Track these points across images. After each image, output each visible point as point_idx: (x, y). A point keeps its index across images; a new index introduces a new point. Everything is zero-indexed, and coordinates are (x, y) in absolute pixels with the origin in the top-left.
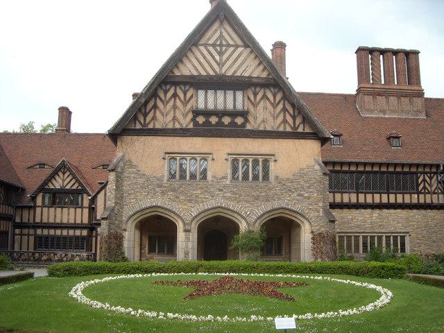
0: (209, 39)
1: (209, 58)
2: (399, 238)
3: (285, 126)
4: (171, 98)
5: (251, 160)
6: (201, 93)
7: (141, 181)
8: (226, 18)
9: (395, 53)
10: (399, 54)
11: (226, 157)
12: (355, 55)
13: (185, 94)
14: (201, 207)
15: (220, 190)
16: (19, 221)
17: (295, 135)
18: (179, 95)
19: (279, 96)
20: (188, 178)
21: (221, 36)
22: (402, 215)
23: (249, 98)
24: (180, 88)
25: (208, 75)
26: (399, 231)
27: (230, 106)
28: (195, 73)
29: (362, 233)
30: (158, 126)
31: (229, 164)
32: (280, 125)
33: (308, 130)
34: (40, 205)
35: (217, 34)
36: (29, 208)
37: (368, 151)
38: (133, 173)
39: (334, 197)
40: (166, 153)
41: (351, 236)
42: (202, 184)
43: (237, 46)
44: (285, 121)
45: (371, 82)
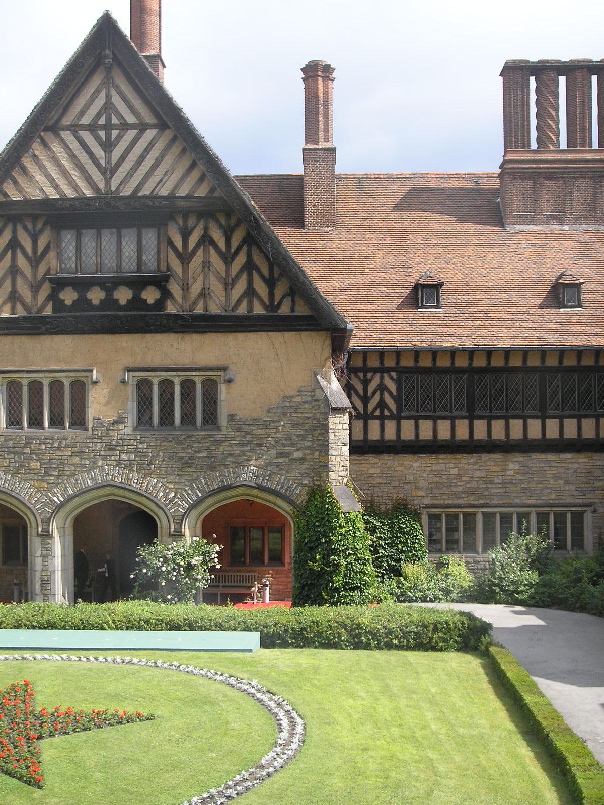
0: (82, 113)
1: (83, 157)
2: (569, 515)
3: (250, 304)
6: (68, 238)
12: (501, 78)
15: (110, 450)
17: (272, 323)
18: (23, 243)
21: (108, 107)
22: (576, 466)
23: (171, 243)
24: (25, 228)
25: (82, 199)
26: (569, 500)
27: (129, 265)
29: (482, 506)
31: (131, 392)
32: (239, 302)
33: (302, 310)
37: (500, 320)
39: (417, 427)
41: (456, 516)
43: (143, 127)
44: (250, 293)
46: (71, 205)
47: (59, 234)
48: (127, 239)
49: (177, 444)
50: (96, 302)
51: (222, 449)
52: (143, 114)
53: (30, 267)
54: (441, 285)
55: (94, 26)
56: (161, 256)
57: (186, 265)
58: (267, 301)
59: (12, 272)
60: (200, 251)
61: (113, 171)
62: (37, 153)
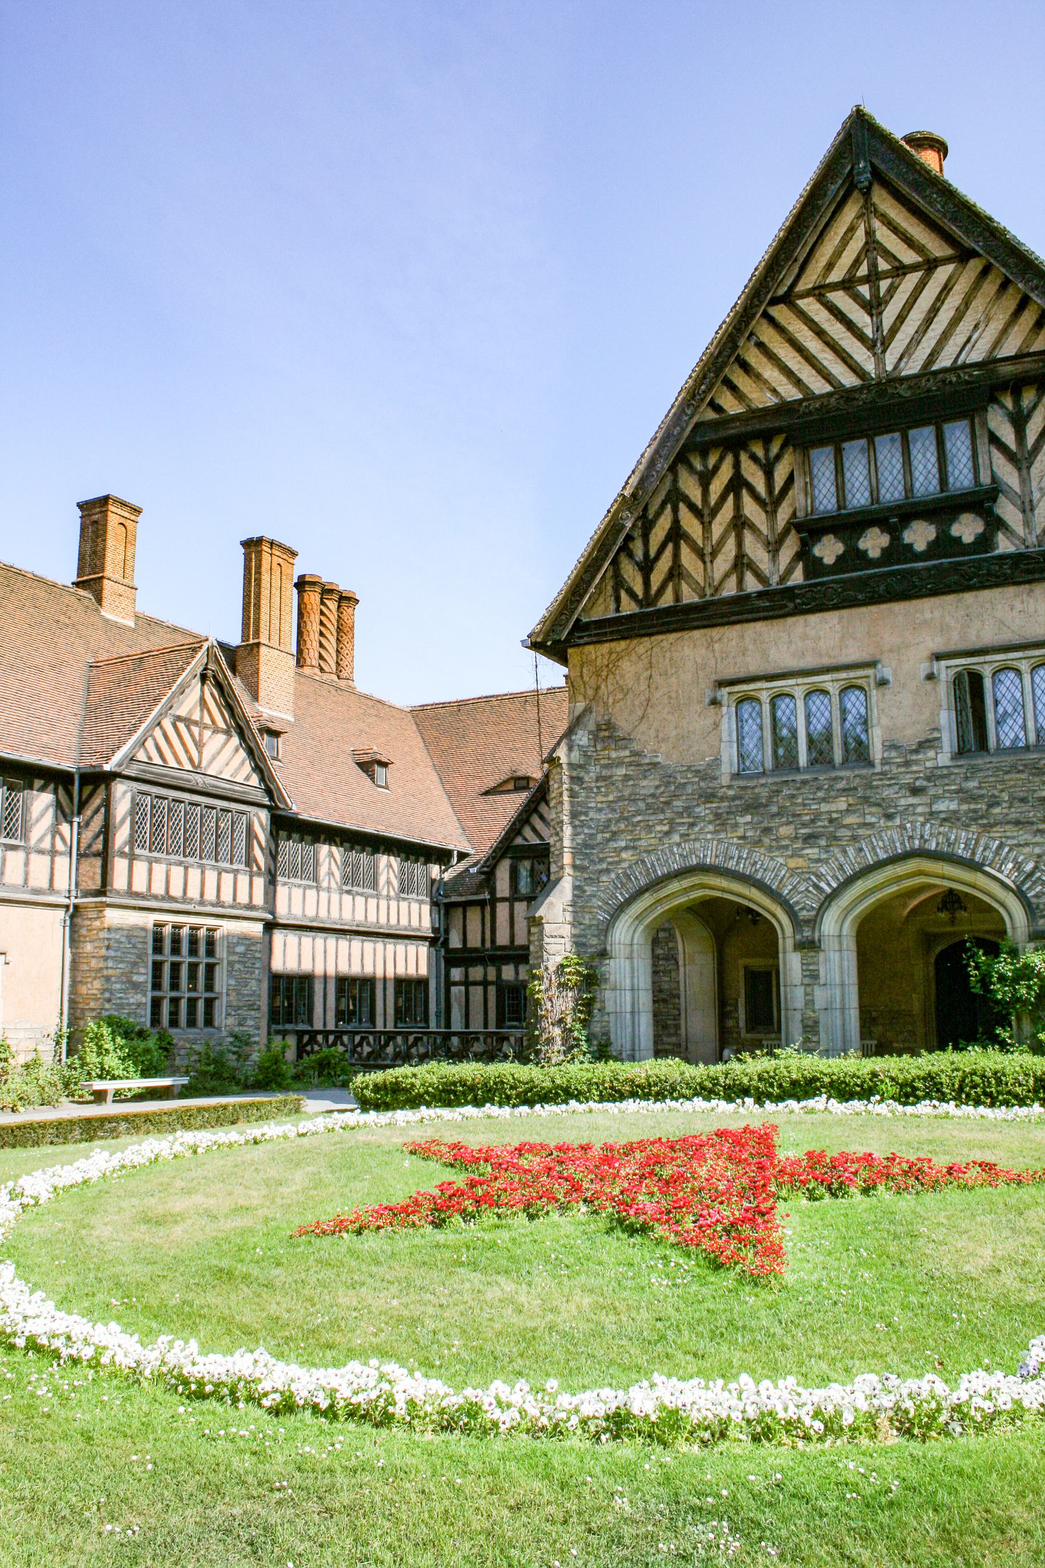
0: (830, 266)
1: (836, 330)
4: (723, 498)
6: (823, 461)
7: (648, 784)
8: (878, 177)
11: (924, 668)
14: (851, 860)
15: (915, 791)
16: (459, 946)
18: (750, 479)
20: (803, 759)
21: (872, 245)
23: (994, 440)
24: (754, 458)
27: (926, 483)
28: (791, 393)
30: (689, 597)
31: (943, 691)
34: (506, 893)
36: (482, 904)
38: (620, 763)
40: (721, 684)
43: (930, 265)
46: (822, 405)
47: (806, 456)
48: (919, 445)
49: (1034, 775)
50: (874, 553)
52: (929, 246)
53: (763, 515)
55: (839, 134)
56: (980, 461)
57: (1024, 471)
59: (735, 525)
62: (764, 339)
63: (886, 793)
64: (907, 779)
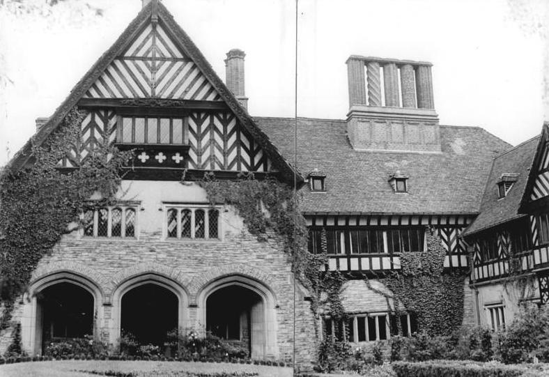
0: (138, 50)
5: (193, 210)
6: (127, 122)
8: (160, 22)
9: (400, 65)
10: (406, 67)
11: (159, 206)
12: (346, 65)
13: (106, 123)
14: (128, 273)
15: (151, 251)
19: (230, 128)
23: (191, 129)
25: (139, 100)
28: (119, 96)
32: (232, 164)
35: (149, 44)
42: (129, 241)
43: (175, 60)
44: (239, 159)
45: (368, 104)
50: (143, 161)
51: (222, 252)
54: (325, 177)
58: (249, 164)
60: (209, 133)
61: (156, 84)
63: (140, 249)
64: (149, 245)
